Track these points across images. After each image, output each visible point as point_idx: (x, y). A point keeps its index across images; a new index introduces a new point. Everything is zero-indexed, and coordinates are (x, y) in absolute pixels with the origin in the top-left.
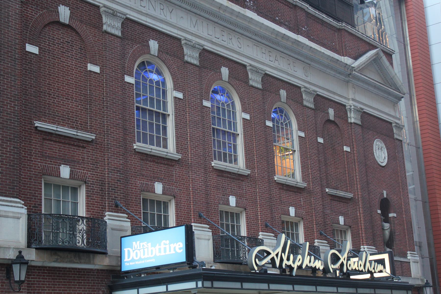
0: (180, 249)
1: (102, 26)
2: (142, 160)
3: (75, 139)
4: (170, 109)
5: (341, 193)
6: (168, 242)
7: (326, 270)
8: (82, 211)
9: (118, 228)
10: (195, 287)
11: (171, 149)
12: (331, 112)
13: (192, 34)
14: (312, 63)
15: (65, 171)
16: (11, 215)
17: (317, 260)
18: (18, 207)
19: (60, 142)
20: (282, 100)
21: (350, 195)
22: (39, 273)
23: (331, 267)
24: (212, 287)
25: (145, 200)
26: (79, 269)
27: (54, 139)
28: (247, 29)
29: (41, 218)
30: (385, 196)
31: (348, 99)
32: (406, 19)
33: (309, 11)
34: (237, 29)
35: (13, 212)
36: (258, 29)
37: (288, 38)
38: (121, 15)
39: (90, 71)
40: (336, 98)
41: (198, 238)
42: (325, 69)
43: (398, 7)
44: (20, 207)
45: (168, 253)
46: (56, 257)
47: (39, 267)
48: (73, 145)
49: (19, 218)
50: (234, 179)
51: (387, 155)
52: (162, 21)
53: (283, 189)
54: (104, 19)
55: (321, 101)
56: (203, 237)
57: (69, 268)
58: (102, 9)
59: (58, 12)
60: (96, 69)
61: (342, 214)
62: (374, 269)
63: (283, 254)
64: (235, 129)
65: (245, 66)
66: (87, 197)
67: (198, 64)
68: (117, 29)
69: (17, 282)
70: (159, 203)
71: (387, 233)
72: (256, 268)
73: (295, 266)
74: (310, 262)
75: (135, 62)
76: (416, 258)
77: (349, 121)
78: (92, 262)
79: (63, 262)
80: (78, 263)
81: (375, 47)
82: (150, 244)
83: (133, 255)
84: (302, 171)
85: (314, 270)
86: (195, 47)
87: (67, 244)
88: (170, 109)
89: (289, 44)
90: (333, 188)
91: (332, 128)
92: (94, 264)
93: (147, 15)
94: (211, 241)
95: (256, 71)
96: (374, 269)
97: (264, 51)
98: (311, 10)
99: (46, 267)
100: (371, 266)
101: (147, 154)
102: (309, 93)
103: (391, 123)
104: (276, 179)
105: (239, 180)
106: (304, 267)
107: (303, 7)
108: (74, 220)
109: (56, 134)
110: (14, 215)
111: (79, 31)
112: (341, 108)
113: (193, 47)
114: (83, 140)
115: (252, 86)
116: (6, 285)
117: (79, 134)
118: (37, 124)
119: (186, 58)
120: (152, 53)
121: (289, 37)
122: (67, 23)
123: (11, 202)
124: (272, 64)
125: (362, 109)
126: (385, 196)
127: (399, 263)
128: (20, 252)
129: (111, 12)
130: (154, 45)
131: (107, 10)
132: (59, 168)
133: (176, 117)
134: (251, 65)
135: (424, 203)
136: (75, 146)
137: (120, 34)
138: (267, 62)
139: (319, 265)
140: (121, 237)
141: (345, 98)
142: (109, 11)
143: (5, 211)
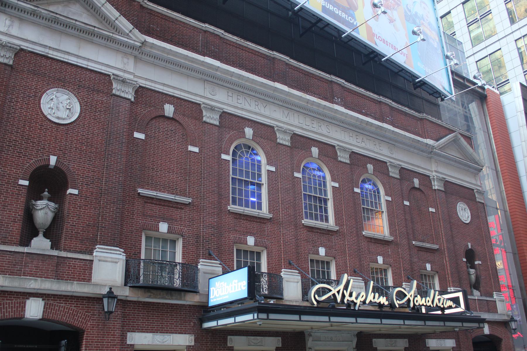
0: (244, 286)
1: (202, 118)
2: (236, 218)
3: (174, 202)
4: (264, 179)
5: (428, 245)
6: (236, 281)
7: (392, 305)
8: (179, 259)
9: (210, 272)
10: (252, 318)
11: (265, 211)
12: (416, 182)
13: (284, 123)
14: (396, 144)
15: (163, 227)
16: (110, 260)
17: (382, 297)
18: (116, 254)
19: (160, 205)
20: (369, 172)
21: (436, 247)
22: (134, 306)
23: (397, 303)
24: (268, 319)
25: (238, 251)
26: (172, 304)
27: (155, 202)
28: (333, 118)
29: (140, 263)
30: (470, 247)
31: (432, 171)
32: (488, 114)
33: (392, 105)
34: (325, 119)
35: (111, 258)
36: (344, 118)
37: (372, 124)
38: (218, 110)
39: (191, 151)
40: (421, 171)
41: (287, 281)
42: (409, 148)
43: (481, 107)
44: (118, 254)
45: (237, 290)
46: (149, 294)
47: (135, 301)
48: (172, 207)
49: (116, 263)
50: (323, 234)
51: (470, 214)
52: (256, 113)
53: (371, 242)
54: (204, 113)
55: (406, 174)
56: (292, 280)
57: (163, 303)
58: (202, 106)
59: (164, 109)
60: (196, 150)
61: (429, 262)
62: (443, 304)
63: (345, 291)
64: (326, 194)
65: (334, 147)
66: (184, 247)
67: (290, 145)
68: (215, 120)
69: (106, 312)
70: (252, 252)
71: (473, 277)
72: (315, 303)
73: (358, 302)
74: (374, 298)
75: (231, 144)
76: (501, 298)
77: (434, 188)
78: (183, 298)
79: (156, 298)
80: (170, 299)
81: (453, 132)
82: (226, 284)
83: (215, 293)
84: (390, 228)
85: (380, 305)
86: (286, 132)
87: (155, 283)
88: (264, 179)
89: (373, 129)
90: (420, 241)
91: (418, 193)
92: (185, 300)
93: (242, 109)
94: (300, 284)
95: (344, 150)
96: (443, 304)
97: (351, 135)
98: (394, 105)
99: (141, 302)
100: (439, 302)
101: (241, 214)
102: (394, 166)
103: (473, 190)
104: (364, 234)
105: (328, 234)
106: (367, 302)
107: (386, 102)
108: (173, 264)
109: (157, 199)
110: (113, 260)
111: (182, 122)
112: (425, 179)
113: (285, 132)
114: (181, 203)
115: (341, 162)
116: (102, 315)
117: (176, 198)
118: (140, 191)
119: (278, 141)
120: (247, 137)
122: (171, 116)
123: (111, 250)
124: (359, 145)
125: (445, 178)
126: (470, 247)
127: (485, 302)
128: (111, 289)
129: (210, 107)
130: (249, 132)
131: (206, 106)
132: (158, 225)
133: (269, 185)
134: (338, 145)
135: (514, 254)
136: (175, 208)
137: (218, 124)
138: (354, 143)
139: (383, 300)
140: (210, 279)
141: (429, 170)
142: (208, 107)
143: (104, 257)
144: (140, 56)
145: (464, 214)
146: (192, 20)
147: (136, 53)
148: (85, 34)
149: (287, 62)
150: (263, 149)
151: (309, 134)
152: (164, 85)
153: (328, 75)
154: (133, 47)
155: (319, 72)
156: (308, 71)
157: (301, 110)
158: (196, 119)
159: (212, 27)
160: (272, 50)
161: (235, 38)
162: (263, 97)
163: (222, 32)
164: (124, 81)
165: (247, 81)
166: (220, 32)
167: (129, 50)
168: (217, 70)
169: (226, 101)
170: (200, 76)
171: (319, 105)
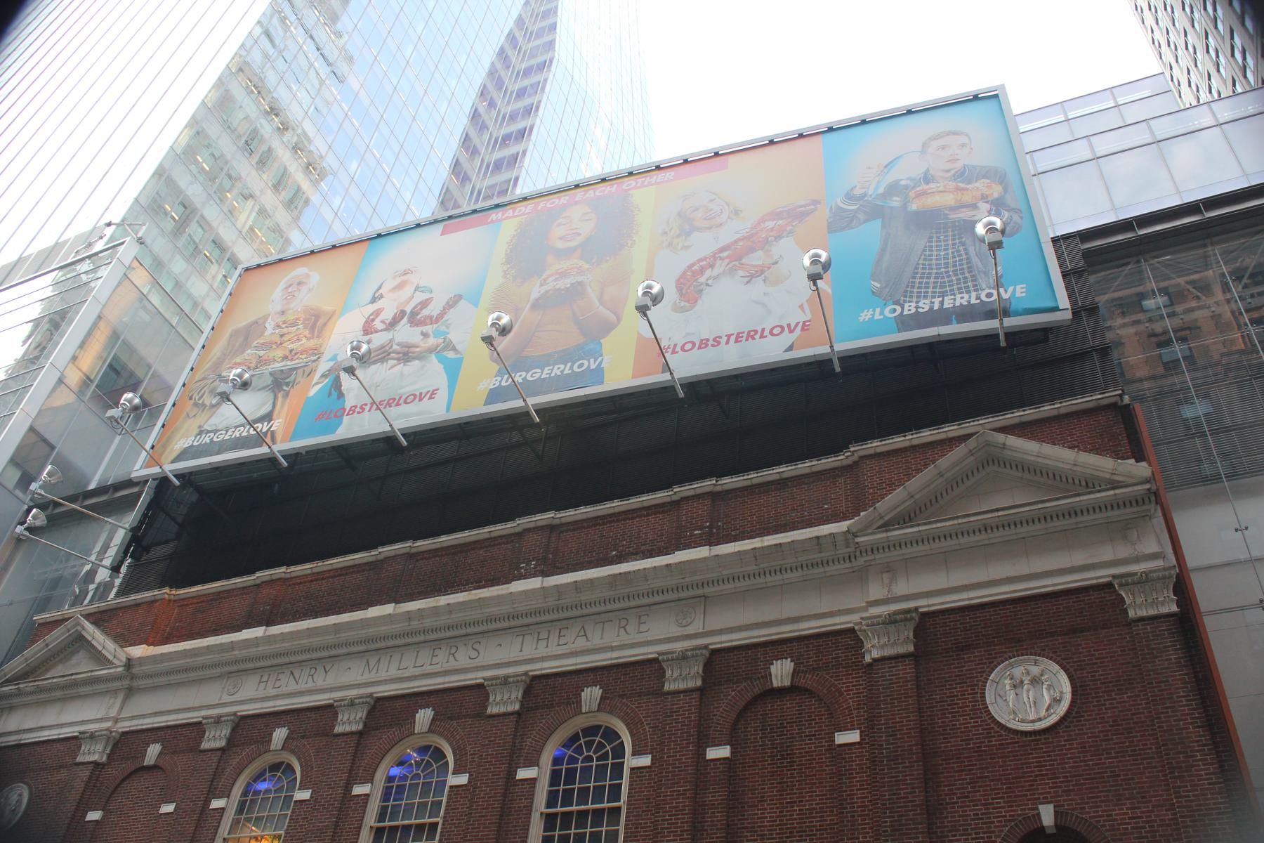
14: (707, 590)
33: (726, 487)
34: (470, 630)
98: (729, 482)
107: (699, 491)
115: (491, 716)
121: (591, 580)
144: (135, 684)
145: (1028, 695)
146: (238, 580)
147: (126, 683)
148: (73, 691)
149: (413, 551)
150: (299, 759)
151: (416, 683)
152: (156, 714)
153: (510, 525)
154: (120, 677)
155: (487, 529)
156: (462, 541)
157: (391, 643)
158: (191, 750)
159: (267, 572)
160: (375, 547)
161: (308, 566)
162: (325, 654)
163: (283, 569)
164: (92, 737)
165: (283, 641)
166: (279, 571)
167: (117, 684)
168: (233, 649)
169: (261, 693)
170: (218, 671)
171: (436, 611)
